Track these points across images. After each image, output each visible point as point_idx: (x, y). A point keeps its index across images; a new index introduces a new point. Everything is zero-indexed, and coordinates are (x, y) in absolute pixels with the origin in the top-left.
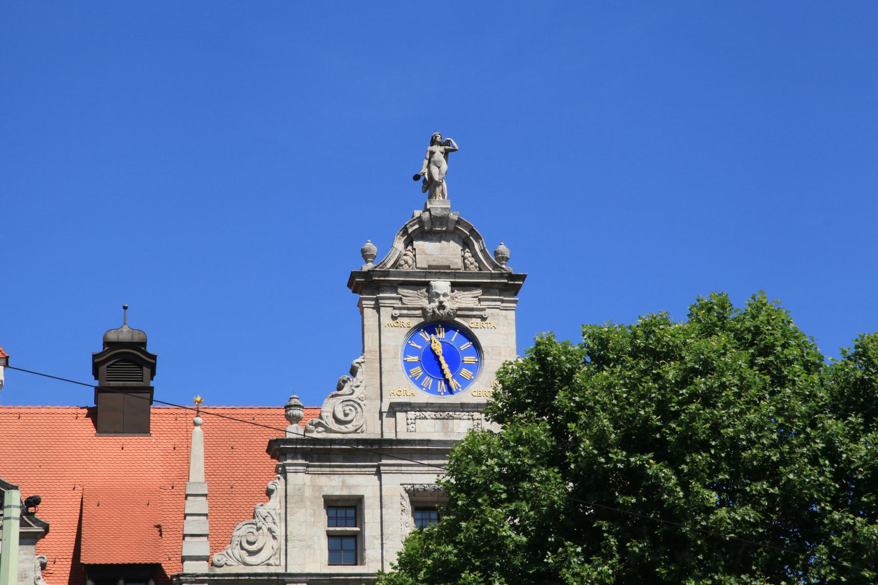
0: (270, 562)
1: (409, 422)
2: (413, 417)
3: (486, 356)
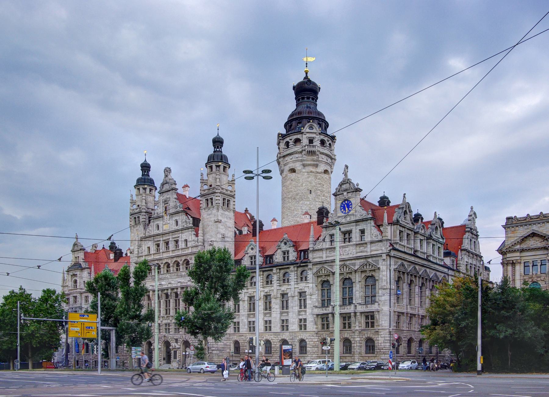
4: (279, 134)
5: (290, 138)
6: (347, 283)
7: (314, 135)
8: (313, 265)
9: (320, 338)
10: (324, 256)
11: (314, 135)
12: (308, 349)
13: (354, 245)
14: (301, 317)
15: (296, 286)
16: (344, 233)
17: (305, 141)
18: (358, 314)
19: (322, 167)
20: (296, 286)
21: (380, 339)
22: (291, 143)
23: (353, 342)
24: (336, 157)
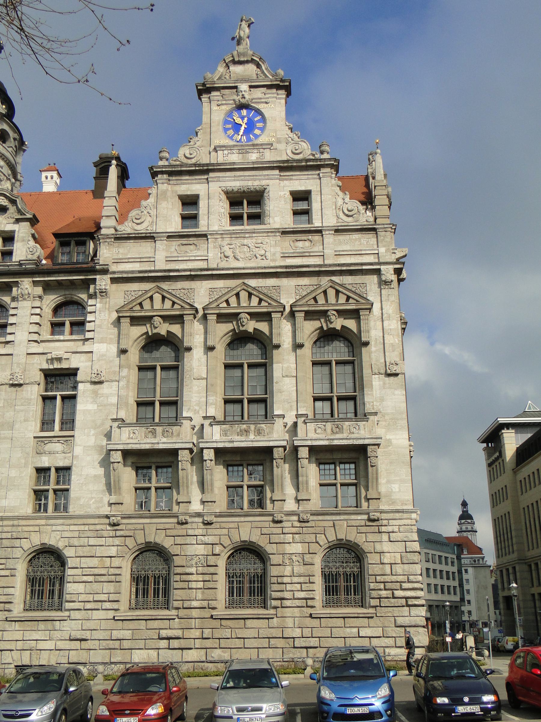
0: (148, 229)
1: (225, 155)
2: (227, 153)
3: (268, 121)
6: (250, 344)
8: (114, 280)
9: (130, 542)
10: (162, 256)
12: (69, 588)
13: (274, 231)
14: (45, 462)
15: (35, 348)
16: (235, 199)
18: (304, 453)
20: (35, 348)
21: (386, 547)
23: (274, 559)
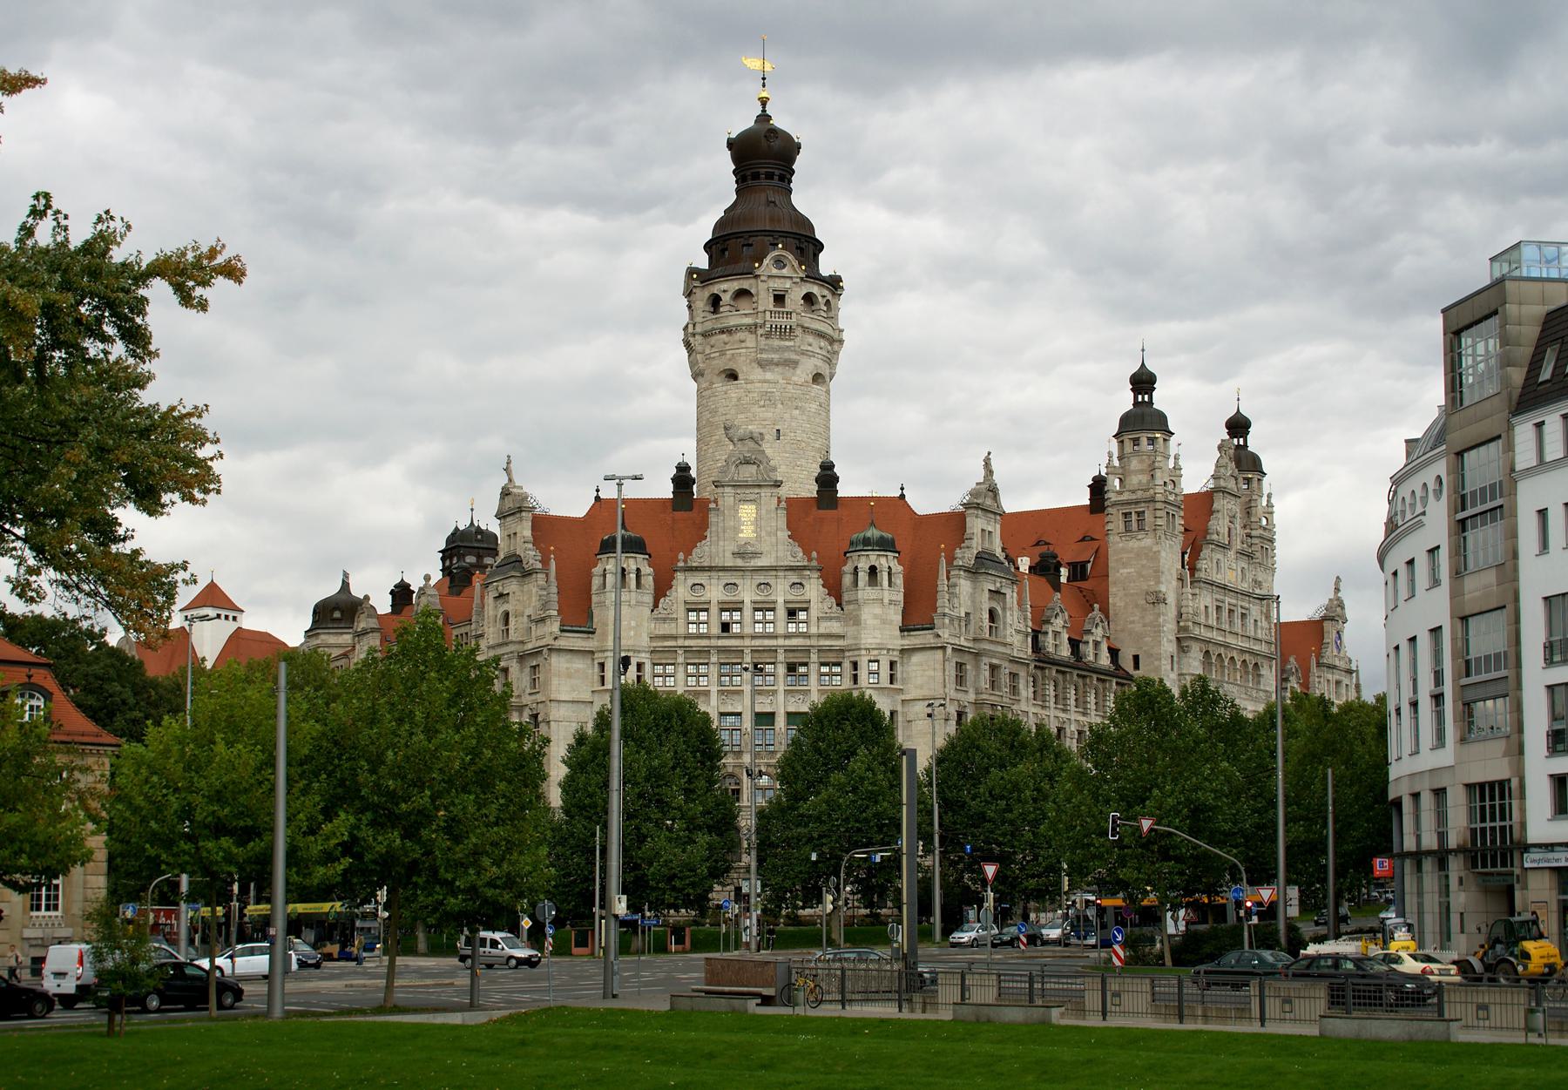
4: (691, 271)
5: (724, 286)
7: (788, 284)
11: (788, 284)
17: (766, 302)
19: (808, 366)
22: (726, 298)
24: (845, 336)
